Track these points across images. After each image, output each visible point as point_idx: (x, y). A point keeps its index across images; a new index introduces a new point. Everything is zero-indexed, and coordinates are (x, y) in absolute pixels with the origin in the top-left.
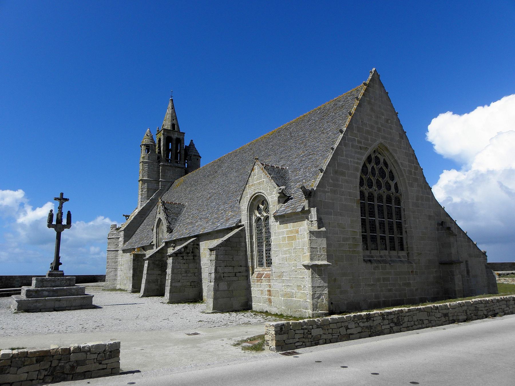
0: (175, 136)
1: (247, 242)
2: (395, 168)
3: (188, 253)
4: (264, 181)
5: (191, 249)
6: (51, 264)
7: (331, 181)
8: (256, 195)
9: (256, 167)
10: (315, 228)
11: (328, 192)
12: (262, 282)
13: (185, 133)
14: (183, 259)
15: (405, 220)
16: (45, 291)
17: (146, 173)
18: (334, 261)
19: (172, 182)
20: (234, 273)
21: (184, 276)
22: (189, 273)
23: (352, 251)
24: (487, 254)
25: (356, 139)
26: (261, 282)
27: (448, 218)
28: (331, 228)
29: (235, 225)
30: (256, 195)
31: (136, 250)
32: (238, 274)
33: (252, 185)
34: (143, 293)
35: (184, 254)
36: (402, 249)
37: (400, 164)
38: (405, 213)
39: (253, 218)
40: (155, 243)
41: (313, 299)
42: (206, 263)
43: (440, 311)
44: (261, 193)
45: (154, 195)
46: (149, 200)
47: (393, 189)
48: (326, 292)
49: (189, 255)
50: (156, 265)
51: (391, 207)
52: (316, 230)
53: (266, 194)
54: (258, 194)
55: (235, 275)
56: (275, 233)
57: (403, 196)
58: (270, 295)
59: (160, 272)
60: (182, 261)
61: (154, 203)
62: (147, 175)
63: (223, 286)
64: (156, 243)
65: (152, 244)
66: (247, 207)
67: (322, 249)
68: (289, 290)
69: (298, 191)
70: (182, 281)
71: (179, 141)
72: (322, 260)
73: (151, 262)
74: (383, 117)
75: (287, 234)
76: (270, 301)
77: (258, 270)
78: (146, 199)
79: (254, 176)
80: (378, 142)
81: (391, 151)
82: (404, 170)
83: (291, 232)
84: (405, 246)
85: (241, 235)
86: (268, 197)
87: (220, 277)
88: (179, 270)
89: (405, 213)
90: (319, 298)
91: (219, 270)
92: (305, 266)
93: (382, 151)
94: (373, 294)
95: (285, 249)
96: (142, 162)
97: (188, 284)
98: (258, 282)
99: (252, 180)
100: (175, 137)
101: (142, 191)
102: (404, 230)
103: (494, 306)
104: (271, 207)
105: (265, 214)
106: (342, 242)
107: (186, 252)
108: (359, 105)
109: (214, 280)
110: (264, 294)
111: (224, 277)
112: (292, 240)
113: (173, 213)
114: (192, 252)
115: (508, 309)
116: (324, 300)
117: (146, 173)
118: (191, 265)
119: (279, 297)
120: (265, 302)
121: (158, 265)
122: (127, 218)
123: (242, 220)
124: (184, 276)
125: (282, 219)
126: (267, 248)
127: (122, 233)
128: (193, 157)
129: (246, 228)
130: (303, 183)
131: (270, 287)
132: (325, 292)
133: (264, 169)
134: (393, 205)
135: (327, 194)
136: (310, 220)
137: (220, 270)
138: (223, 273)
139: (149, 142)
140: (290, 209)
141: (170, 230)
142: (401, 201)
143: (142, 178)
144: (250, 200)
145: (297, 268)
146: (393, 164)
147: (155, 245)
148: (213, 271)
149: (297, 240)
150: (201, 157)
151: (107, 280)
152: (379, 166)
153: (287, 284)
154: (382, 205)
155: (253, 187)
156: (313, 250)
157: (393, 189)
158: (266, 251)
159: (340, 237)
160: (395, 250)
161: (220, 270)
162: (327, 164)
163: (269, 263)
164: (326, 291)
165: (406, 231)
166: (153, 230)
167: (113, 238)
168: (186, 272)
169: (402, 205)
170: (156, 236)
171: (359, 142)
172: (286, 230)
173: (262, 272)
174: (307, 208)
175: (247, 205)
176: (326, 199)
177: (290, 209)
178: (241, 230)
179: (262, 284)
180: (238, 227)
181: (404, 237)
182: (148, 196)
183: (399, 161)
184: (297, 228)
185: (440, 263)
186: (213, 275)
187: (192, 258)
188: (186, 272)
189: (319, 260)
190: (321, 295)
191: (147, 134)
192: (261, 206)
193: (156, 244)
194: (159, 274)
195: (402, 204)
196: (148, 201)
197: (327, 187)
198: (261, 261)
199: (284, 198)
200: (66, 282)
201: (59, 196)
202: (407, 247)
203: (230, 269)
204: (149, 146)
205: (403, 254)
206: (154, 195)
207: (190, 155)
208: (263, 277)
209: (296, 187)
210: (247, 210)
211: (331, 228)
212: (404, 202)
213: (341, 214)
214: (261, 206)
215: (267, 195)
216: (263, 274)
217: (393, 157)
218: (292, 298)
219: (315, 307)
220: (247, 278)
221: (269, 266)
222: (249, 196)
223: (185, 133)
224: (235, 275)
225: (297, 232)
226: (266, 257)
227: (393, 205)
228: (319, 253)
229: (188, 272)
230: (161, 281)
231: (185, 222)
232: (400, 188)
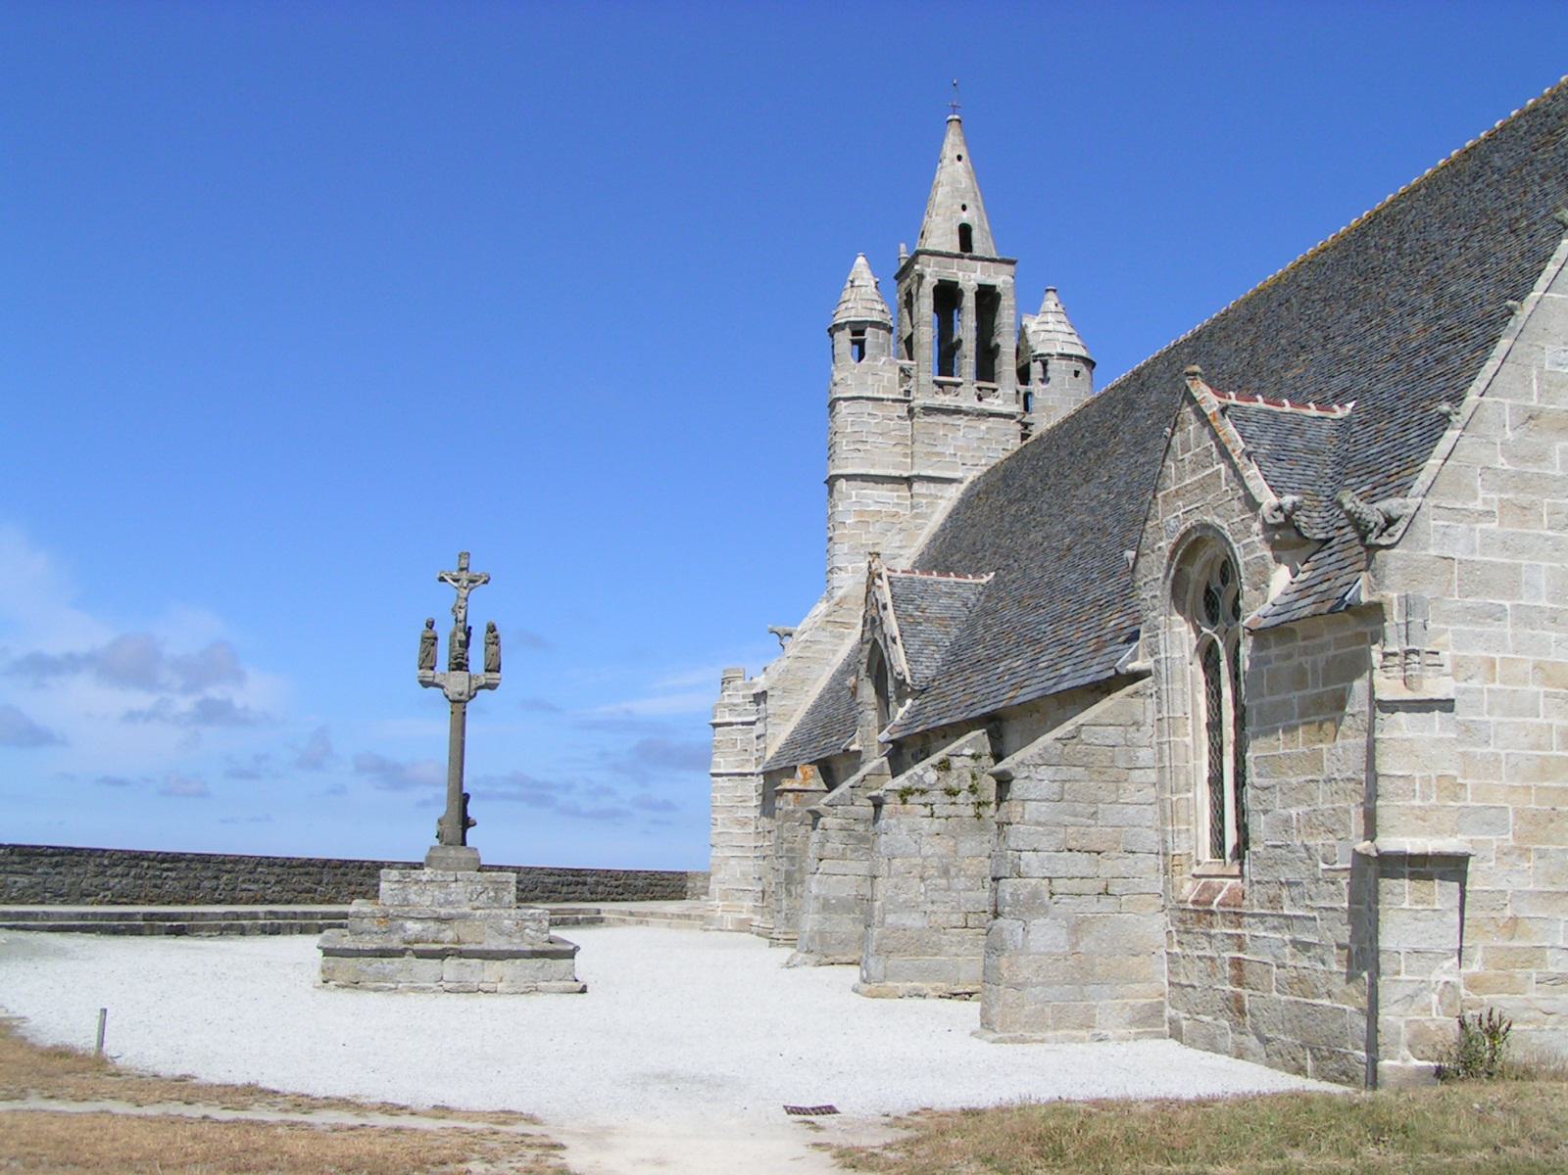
0: (973, 276)
3: (951, 793)
4: (1218, 474)
7: (1501, 463)
12: (1215, 923)
18: (1510, 836)
22: (957, 876)
26: (1211, 925)
28: (1502, 686)
35: (936, 796)
49: (960, 798)
50: (856, 838)
57: (1330, 555)
58: (1239, 981)
67: (1434, 781)
70: (929, 907)
79: (1185, 450)
86: (1235, 546)
88: (914, 861)
91: (1027, 865)
97: (957, 919)
99: (1177, 468)
100: (972, 282)
106: (1560, 753)
107: (941, 785)
112: (1321, 741)
113: (927, 620)
114: (973, 790)
130: (1389, 477)
135: (1479, 526)
137: (1035, 864)
138: (1050, 878)
144: (1172, 558)
145: (1338, 866)
155: (1180, 503)
159: (1551, 726)
161: (1035, 864)
176: (1473, 551)
187: (971, 811)
188: (945, 872)
197: (1481, 494)
203: (1082, 864)
208: (1216, 902)
211: (1502, 686)
213: (1555, 620)
222: (1166, 545)
229: (953, 871)
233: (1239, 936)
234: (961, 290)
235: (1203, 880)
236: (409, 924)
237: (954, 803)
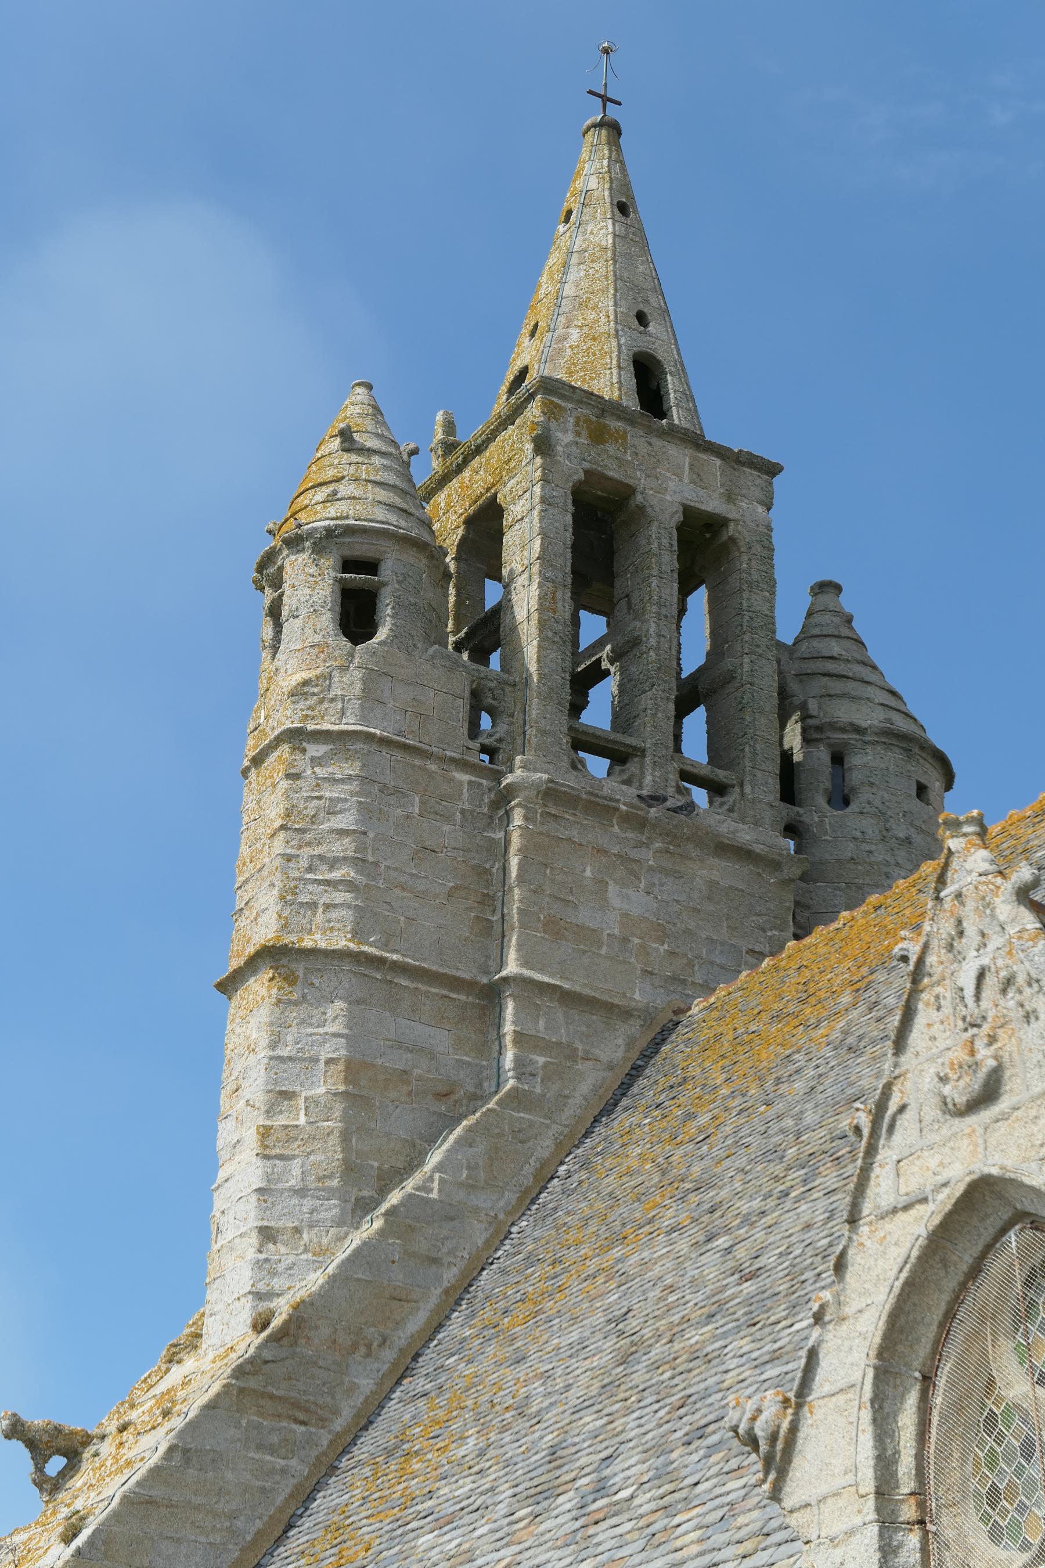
19: (647, 1015)
45: (435, 1158)
46: (372, 1226)
61: (435, 1261)
62: (341, 897)
78: (332, 1209)
96: (296, 737)
117: (336, 875)
122: (56, 1464)
182: (351, 1169)
191: (346, 435)
196: (356, 1239)
204: (371, 567)
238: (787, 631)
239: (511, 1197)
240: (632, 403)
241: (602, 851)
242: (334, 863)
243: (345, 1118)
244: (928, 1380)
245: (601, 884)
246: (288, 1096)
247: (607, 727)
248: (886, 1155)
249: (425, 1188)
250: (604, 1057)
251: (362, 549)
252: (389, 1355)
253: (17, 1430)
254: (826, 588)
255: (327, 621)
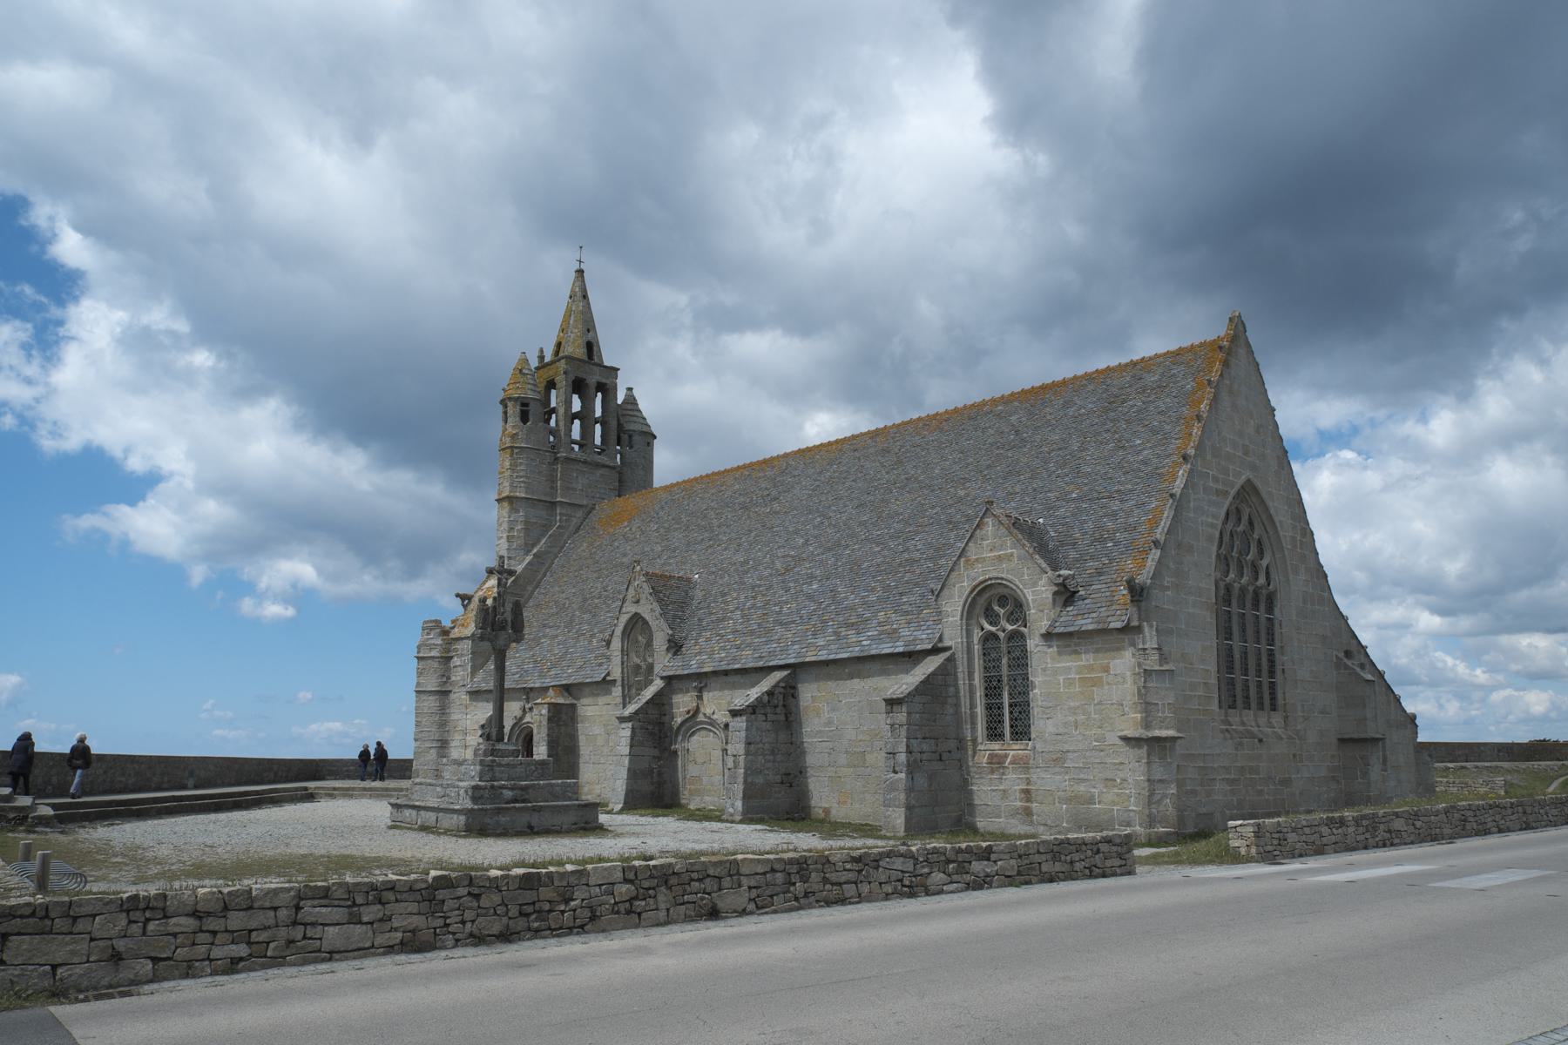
1: (961, 687)
2: (1267, 532)
4: (1012, 555)
5: (781, 697)
6: (483, 727)
8: (987, 583)
9: (989, 521)
10: (1153, 662)
11: (1168, 588)
13: (619, 369)
14: (766, 721)
15: (1282, 647)
16: (506, 788)
17: (522, 479)
20: (938, 754)
21: (769, 761)
23: (1204, 710)
24: (1417, 722)
25: (1211, 473)
27: (1354, 641)
29: (930, 647)
30: (989, 582)
31: (551, 693)
32: (945, 756)
33: (977, 560)
34: (622, 802)
36: (1274, 708)
37: (1278, 524)
38: (1283, 631)
39: (975, 635)
40: (616, 674)
41: (1150, 803)
42: (820, 732)
43: (1421, 818)
44: (1002, 579)
45: (543, 541)
47: (1262, 580)
48: (1174, 791)
49: (778, 710)
51: (1257, 617)
52: (1157, 668)
53: (1018, 583)
54: (993, 582)
55: (940, 755)
56: (1044, 670)
59: (656, 752)
60: (764, 724)
63: (921, 781)
64: (623, 678)
65: (608, 678)
66: (960, 609)
68: (1082, 789)
69: (1097, 582)
71: (607, 389)
72: (1167, 728)
73: (638, 724)
74: (1252, 422)
75: (1077, 674)
76: (1028, 812)
77: (987, 748)
78: (522, 553)
80: (1244, 478)
81: (1264, 496)
82: (1285, 536)
83: (1090, 668)
84: (1280, 701)
85: (946, 672)
86: (1025, 591)
87: (915, 761)
89: (1283, 631)
90: (1159, 802)
92: (1126, 739)
93: (1248, 497)
94: (1235, 799)
95: (1072, 704)
96: (511, 447)
97: (779, 779)
98: (992, 772)
101: (511, 529)
102: (1278, 668)
103: (1486, 816)
104: (1032, 612)
105: (1010, 627)
108: (1215, 400)
109: (905, 769)
110: (1012, 798)
111: (921, 761)
112: (1093, 686)
113: (671, 603)
115: (1503, 822)
116: (1168, 808)
117: (522, 479)
118: (783, 736)
119: (1054, 803)
120: (1013, 816)
121: (651, 734)
123: (946, 636)
124: (769, 761)
125: (1048, 636)
126: (1013, 700)
127: (466, 646)
128: (636, 438)
129: (959, 656)
131: (1028, 784)
132: (1172, 792)
133: (1012, 528)
134: (1263, 615)
136: (1141, 646)
137: (915, 745)
139: (529, 392)
140: (1090, 620)
141: (675, 647)
142: (1275, 603)
143: (511, 492)
146: (1263, 524)
147: (619, 683)
148: (902, 748)
149: (1106, 687)
150: (655, 437)
151: (417, 770)
152: (1241, 528)
153: (1076, 777)
154: (1244, 614)
155: (980, 566)
156: (1147, 707)
157: (1262, 580)
158: (1011, 706)
160: (1250, 709)
162: (1166, 530)
163: (1021, 732)
164: (1173, 790)
165: (1283, 669)
166: (608, 643)
167: (433, 657)
168: (773, 752)
169: (1276, 614)
170: (622, 658)
171: (1216, 480)
172: (1075, 664)
173: (1000, 752)
174: (1135, 623)
175: (961, 603)
177: (1090, 620)
178: (948, 660)
179: (1004, 777)
180: (936, 650)
181: (1278, 682)
183: (1276, 519)
184: (1106, 661)
185: (1339, 739)
186: (902, 758)
187: (782, 718)
189: (1161, 728)
190: (1164, 796)
192: (996, 608)
193: (623, 680)
194: (654, 757)
195: (1277, 610)
198: (996, 728)
199: (1066, 595)
200: (536, 768)
201: (494, 564)
202: (1285, 704)
205: (1277, 719)
206: (543, 541)
207: (630, 430)
209: (1088, 572)
210: (962, 615)
212: (1281, 608)
214: (996, 608)
215: (1021, 587)
216: (1006, 756)
217: (1267, 509)
218: (1091, 804)
219: (1151, 821)
220: (961, 764)
221: (1017, 740)
223: (619, 369)
224: (940, 755)
225: (1106, 669)
226: (1011, 719)
227: (1263, 615)
228: (1160, 715)
229: (776, 751)
230: (660, 774)
231: (723, 628)
232: (1273, 575)
233: (1028, 778)
234: (587, 384)
235: (988, 752)
236: (504, 791)
237: (776, 714)
238: (619, 401)
239: (558, 548)
240: (585, 357)
241: (577, 470)
242: (521, 477)
243: (525, 533)
244: (629, 635)
245: (577, 477)
246: (513, 528)
247: (579, 439)
248: (625, 605)
249: (541, 548)
250: (577, 515)
251: (525, 401)
252: (535, 583)
253: (458, 595)
254: (630, 389)
255: (518, 419)
